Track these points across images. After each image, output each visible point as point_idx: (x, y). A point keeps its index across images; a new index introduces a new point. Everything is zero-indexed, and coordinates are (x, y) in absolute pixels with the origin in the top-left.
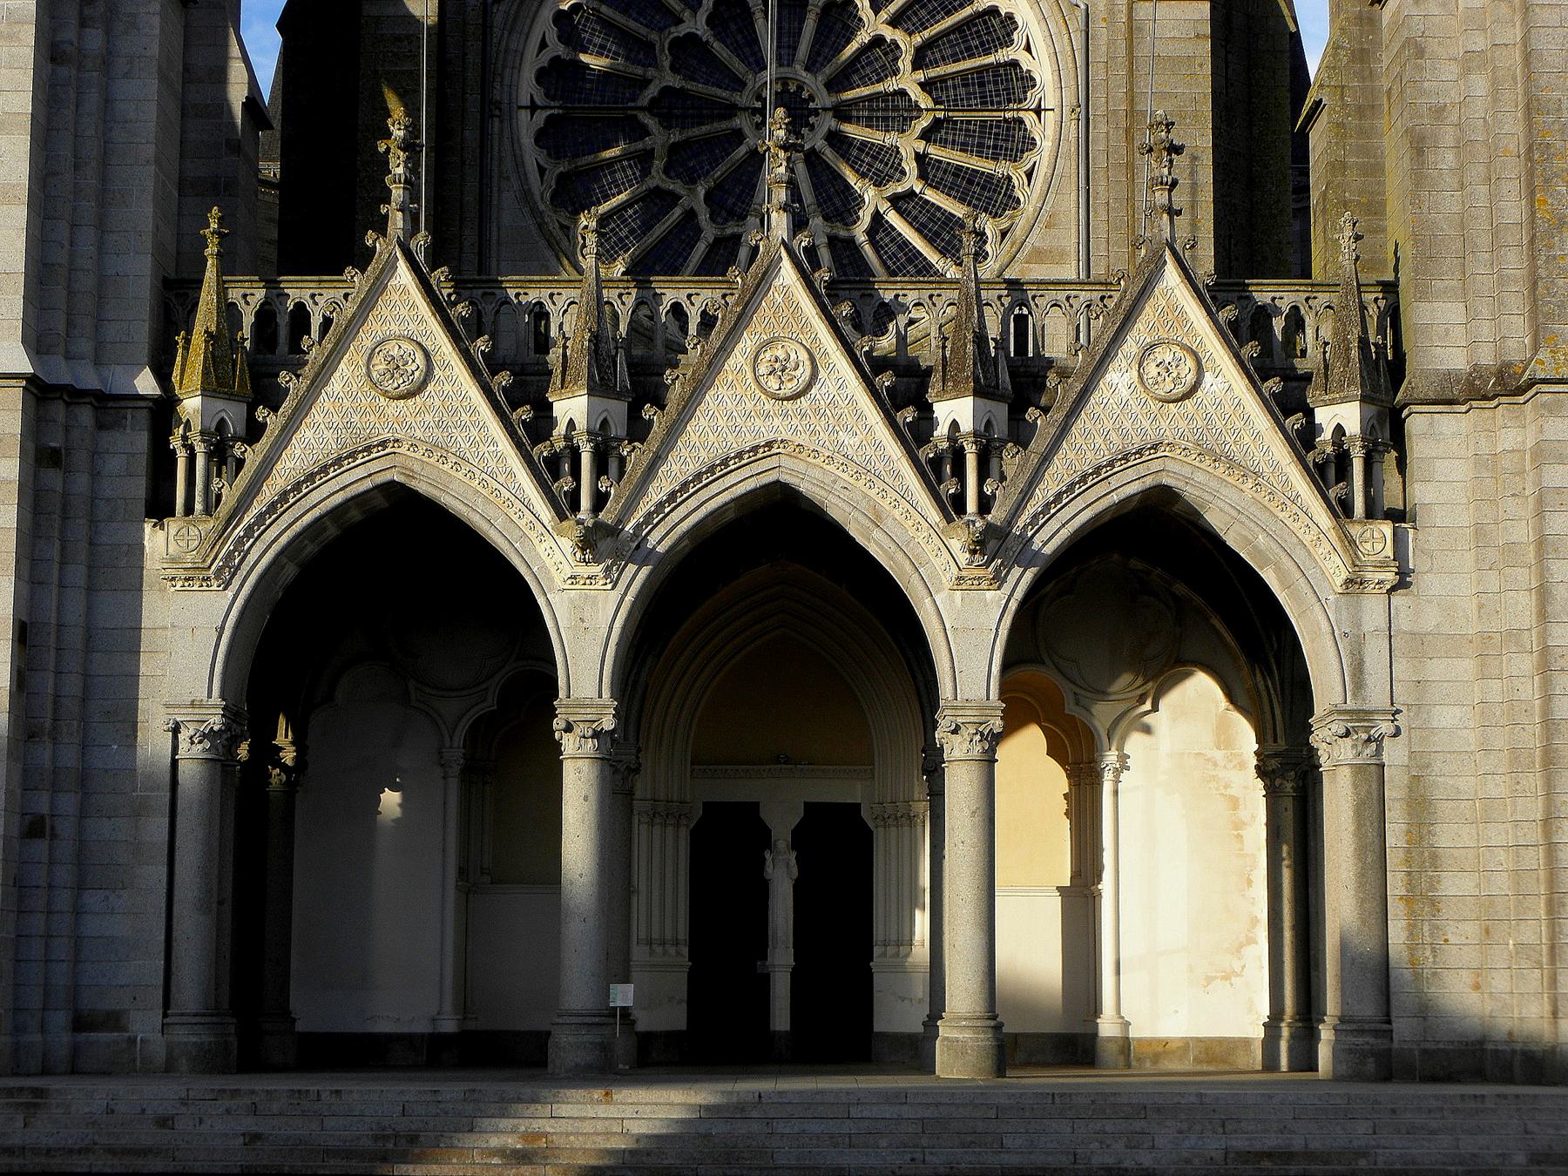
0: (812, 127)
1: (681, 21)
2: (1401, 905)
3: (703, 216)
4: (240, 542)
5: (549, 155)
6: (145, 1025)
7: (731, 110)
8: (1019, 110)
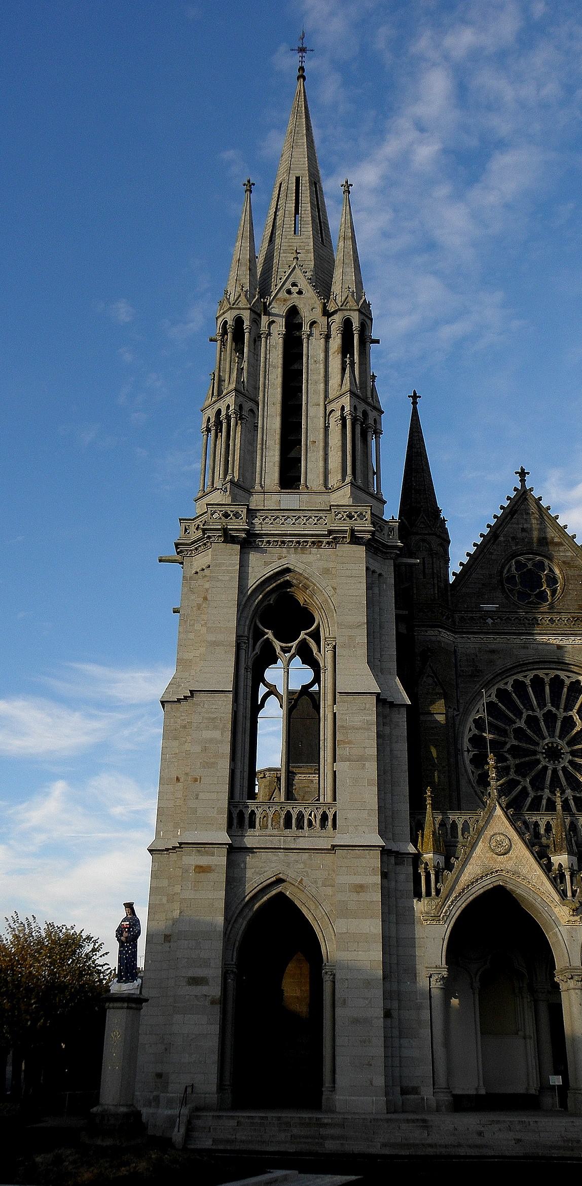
0: (563, 758)
1: (515, 723)
3: (530, 789)
4: (449, 906)
5: (475, 767)
6: (427, 1092)
7: (535, 753)
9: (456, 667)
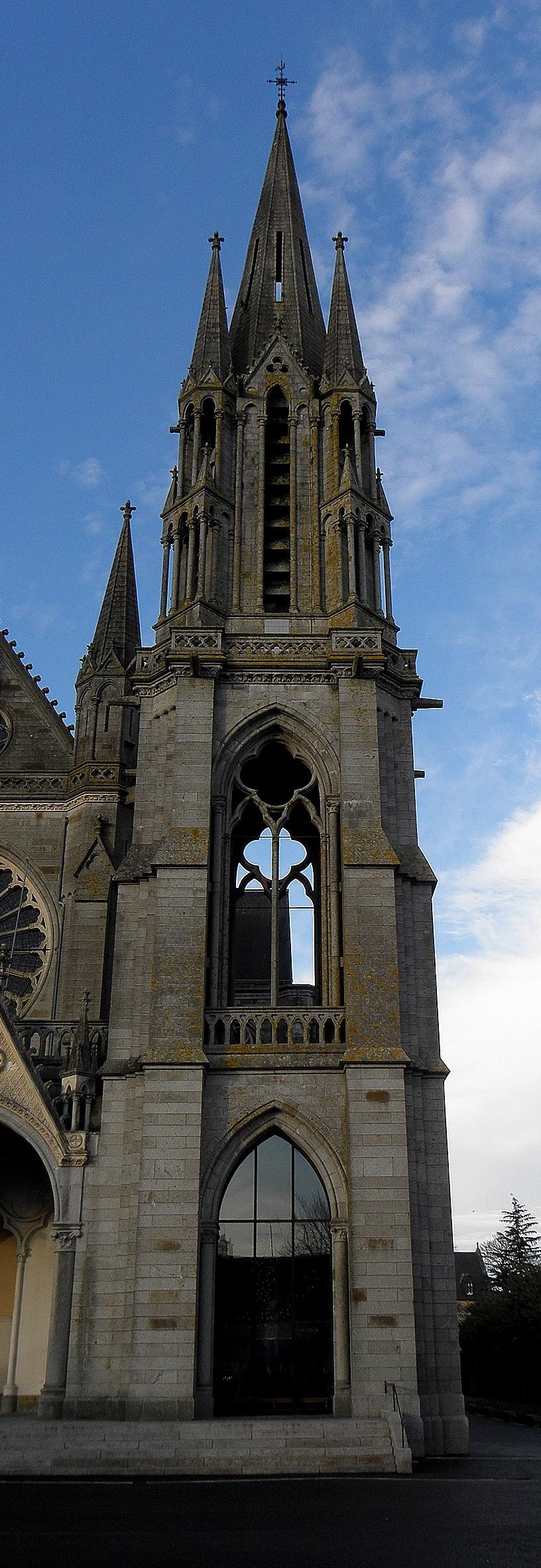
2: (76, 1323)
8: (36, 950)
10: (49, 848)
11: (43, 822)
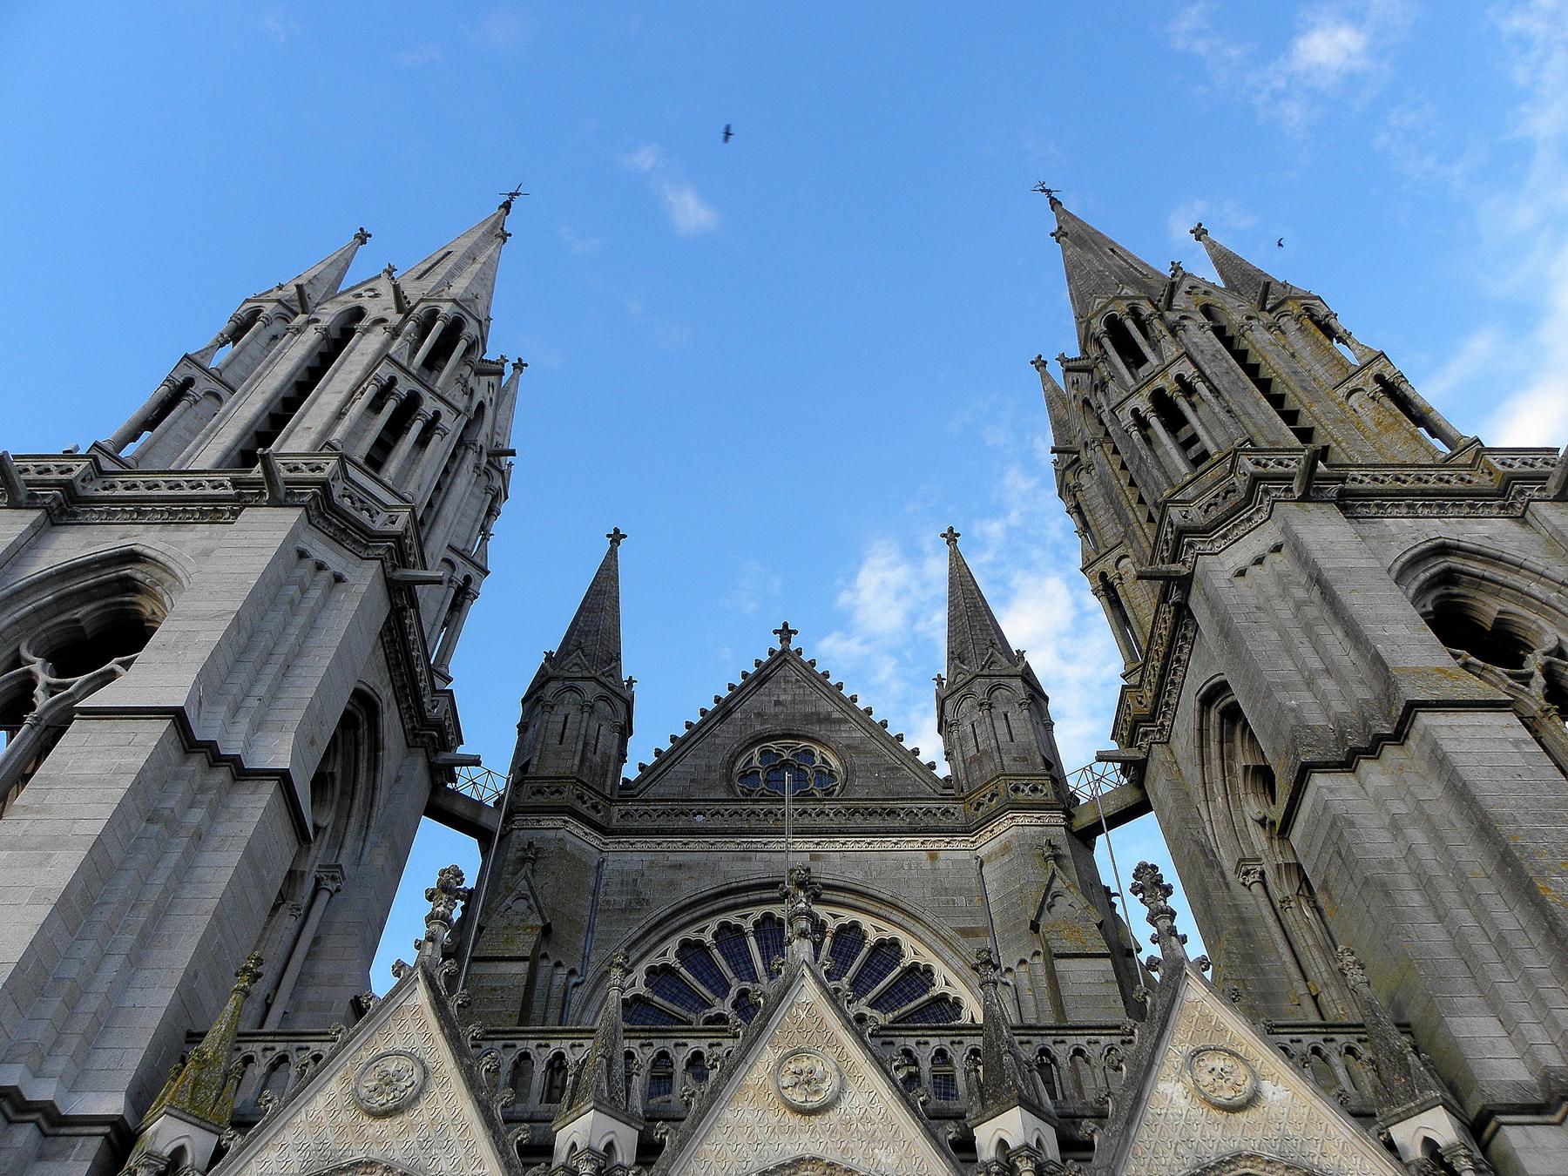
9: (595, 893)
10: (961, 901)
11: (941, 865)
